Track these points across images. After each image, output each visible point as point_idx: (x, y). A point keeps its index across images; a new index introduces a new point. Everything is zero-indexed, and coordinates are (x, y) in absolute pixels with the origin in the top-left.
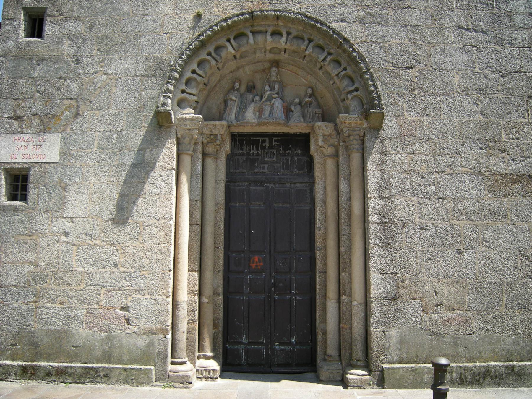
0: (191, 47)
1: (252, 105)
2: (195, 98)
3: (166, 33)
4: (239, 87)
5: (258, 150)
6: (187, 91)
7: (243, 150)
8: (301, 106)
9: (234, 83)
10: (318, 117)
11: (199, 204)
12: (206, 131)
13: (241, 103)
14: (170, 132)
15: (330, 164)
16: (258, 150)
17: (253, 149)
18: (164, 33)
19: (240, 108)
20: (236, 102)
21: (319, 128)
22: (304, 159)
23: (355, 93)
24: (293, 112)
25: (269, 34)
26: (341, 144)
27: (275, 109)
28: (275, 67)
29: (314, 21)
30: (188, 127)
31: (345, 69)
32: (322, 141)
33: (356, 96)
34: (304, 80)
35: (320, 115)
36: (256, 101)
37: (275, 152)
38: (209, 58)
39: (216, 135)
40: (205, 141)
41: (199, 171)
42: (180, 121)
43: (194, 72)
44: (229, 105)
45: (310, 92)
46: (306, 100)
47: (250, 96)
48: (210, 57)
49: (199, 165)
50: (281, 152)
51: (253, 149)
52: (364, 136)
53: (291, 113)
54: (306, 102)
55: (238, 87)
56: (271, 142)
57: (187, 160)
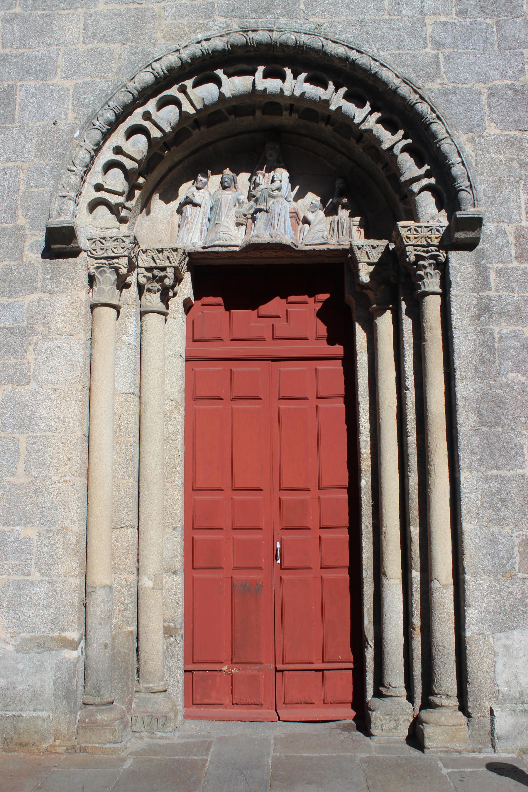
6: (105, 187)
39: (163, 269)
48: (148, 122)
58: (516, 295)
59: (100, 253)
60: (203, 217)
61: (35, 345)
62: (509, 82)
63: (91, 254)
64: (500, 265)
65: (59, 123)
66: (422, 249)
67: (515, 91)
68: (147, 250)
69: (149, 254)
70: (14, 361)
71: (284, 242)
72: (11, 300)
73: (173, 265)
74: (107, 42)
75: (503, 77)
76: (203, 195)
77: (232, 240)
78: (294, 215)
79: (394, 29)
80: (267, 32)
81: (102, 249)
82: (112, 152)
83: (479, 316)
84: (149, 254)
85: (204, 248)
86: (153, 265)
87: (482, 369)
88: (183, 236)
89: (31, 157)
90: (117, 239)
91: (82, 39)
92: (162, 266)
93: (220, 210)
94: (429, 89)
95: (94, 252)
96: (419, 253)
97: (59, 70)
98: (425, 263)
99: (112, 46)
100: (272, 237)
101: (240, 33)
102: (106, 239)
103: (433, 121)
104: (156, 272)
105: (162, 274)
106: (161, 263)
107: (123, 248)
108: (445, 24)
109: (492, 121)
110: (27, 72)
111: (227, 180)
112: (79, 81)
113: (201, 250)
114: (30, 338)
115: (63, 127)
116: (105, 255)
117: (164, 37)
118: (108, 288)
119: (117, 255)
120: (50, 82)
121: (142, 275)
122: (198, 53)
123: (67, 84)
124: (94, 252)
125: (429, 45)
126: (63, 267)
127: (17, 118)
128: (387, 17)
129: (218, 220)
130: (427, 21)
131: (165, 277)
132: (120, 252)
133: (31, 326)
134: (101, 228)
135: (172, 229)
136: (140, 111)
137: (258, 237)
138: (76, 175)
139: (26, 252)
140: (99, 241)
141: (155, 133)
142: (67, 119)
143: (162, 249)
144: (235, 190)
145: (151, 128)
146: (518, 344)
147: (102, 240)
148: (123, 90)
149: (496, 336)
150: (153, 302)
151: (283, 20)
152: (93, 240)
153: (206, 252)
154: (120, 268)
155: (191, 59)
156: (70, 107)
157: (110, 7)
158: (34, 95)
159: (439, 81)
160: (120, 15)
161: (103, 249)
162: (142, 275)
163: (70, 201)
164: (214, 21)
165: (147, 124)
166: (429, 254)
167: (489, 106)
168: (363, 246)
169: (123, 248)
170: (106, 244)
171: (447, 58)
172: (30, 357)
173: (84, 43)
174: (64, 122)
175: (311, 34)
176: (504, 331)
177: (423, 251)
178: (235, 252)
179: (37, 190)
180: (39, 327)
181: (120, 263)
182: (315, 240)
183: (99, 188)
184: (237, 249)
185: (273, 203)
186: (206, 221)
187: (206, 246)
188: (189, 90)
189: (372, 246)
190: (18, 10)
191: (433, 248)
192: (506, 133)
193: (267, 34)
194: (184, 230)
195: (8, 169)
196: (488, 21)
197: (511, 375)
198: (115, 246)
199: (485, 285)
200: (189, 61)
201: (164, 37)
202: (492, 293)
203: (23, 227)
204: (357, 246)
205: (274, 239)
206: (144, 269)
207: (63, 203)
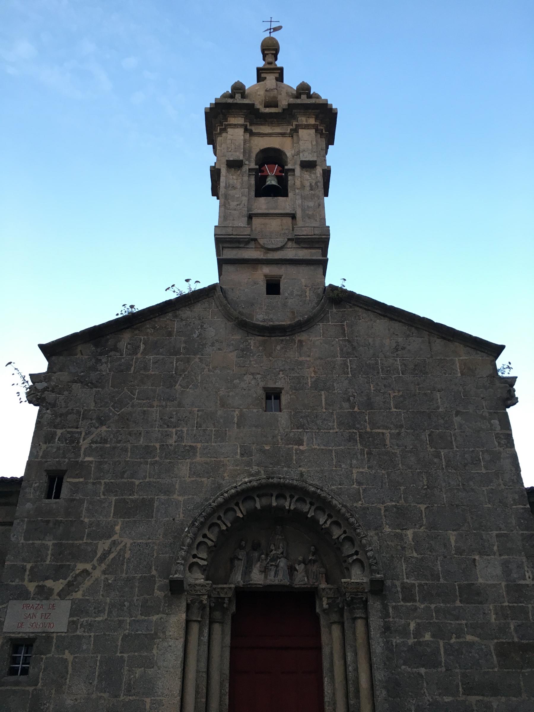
1: (258, 565)
2: (205, 563)
8: (306, 565)
10: (322, 577)
11: (205, 675)
12: (214, 595)
15: (336, 631)
19: (246, 568)
21: (324, 589)
23: (355, 557)
25: (274, 498)
26: (346, 608)
32: (327, 604)
33: (357, 559)
35: (324, 575)
36: (262, 560)
39: (224, 598)
40: (213, 605)
41: (205, 639)
46: (310, 558)
49: (206, 631)
52: (367, 601)
53: (296, 572)
57: (195, 628)
58: (403, 621)
59: (194, 592)
61: (158, 644)
62: (394, 503)
64: (394, 604)
65: (176, 519)
67: (398, 508)
70: (146, 654)
72: (146, 618)
74: (200, 477)
75: (392, 501)
79: (338, 475)
83: (385, 633)
87: (387, 663)
89: (161, 537)
91: (188, 475)
94: (356, 507)
97: (176, 491)
99: (203, 479)
108: (362, 473)
109: (387, 524)
110: (160, 491)
112: (186, 497)
114: (156, 640)
115: (177, 522)
117: (228, 476)
120: (171, 497)
123: (181, 498)
125: (355, 484)
127: (154, 515)
128: (335, 469)
130: (354, 471)
131: (224, 603)
132: (204, 591)
133: (156, 633)
136: (216, 515)
139: (156, 591)
141: (224, 528)
142: (179, 517)
146: (406, 649)
149: (394, 644)
151: (285, 469)
156: (181, 511)
157: (203, 459)
158: (163, 504)
159: (360, 502)
160: (206, 463)
164: (252, 468)
167: (385, 517)
171: (364, 490)
172: (155, 652)
174: (178, 519)
176: (398, 641)
177: (355, 595)
179: (163, 555)
180: (161, 635)
186: (245, 568)
188: (240, 505)
190: (157, 459)
192: (394, 531)
195: (149, 543)
196: (383, 472)
197: (403, 667)
199: (387, 615)
201: (228, 476)
202: (391, 619)
203: (155, 576)
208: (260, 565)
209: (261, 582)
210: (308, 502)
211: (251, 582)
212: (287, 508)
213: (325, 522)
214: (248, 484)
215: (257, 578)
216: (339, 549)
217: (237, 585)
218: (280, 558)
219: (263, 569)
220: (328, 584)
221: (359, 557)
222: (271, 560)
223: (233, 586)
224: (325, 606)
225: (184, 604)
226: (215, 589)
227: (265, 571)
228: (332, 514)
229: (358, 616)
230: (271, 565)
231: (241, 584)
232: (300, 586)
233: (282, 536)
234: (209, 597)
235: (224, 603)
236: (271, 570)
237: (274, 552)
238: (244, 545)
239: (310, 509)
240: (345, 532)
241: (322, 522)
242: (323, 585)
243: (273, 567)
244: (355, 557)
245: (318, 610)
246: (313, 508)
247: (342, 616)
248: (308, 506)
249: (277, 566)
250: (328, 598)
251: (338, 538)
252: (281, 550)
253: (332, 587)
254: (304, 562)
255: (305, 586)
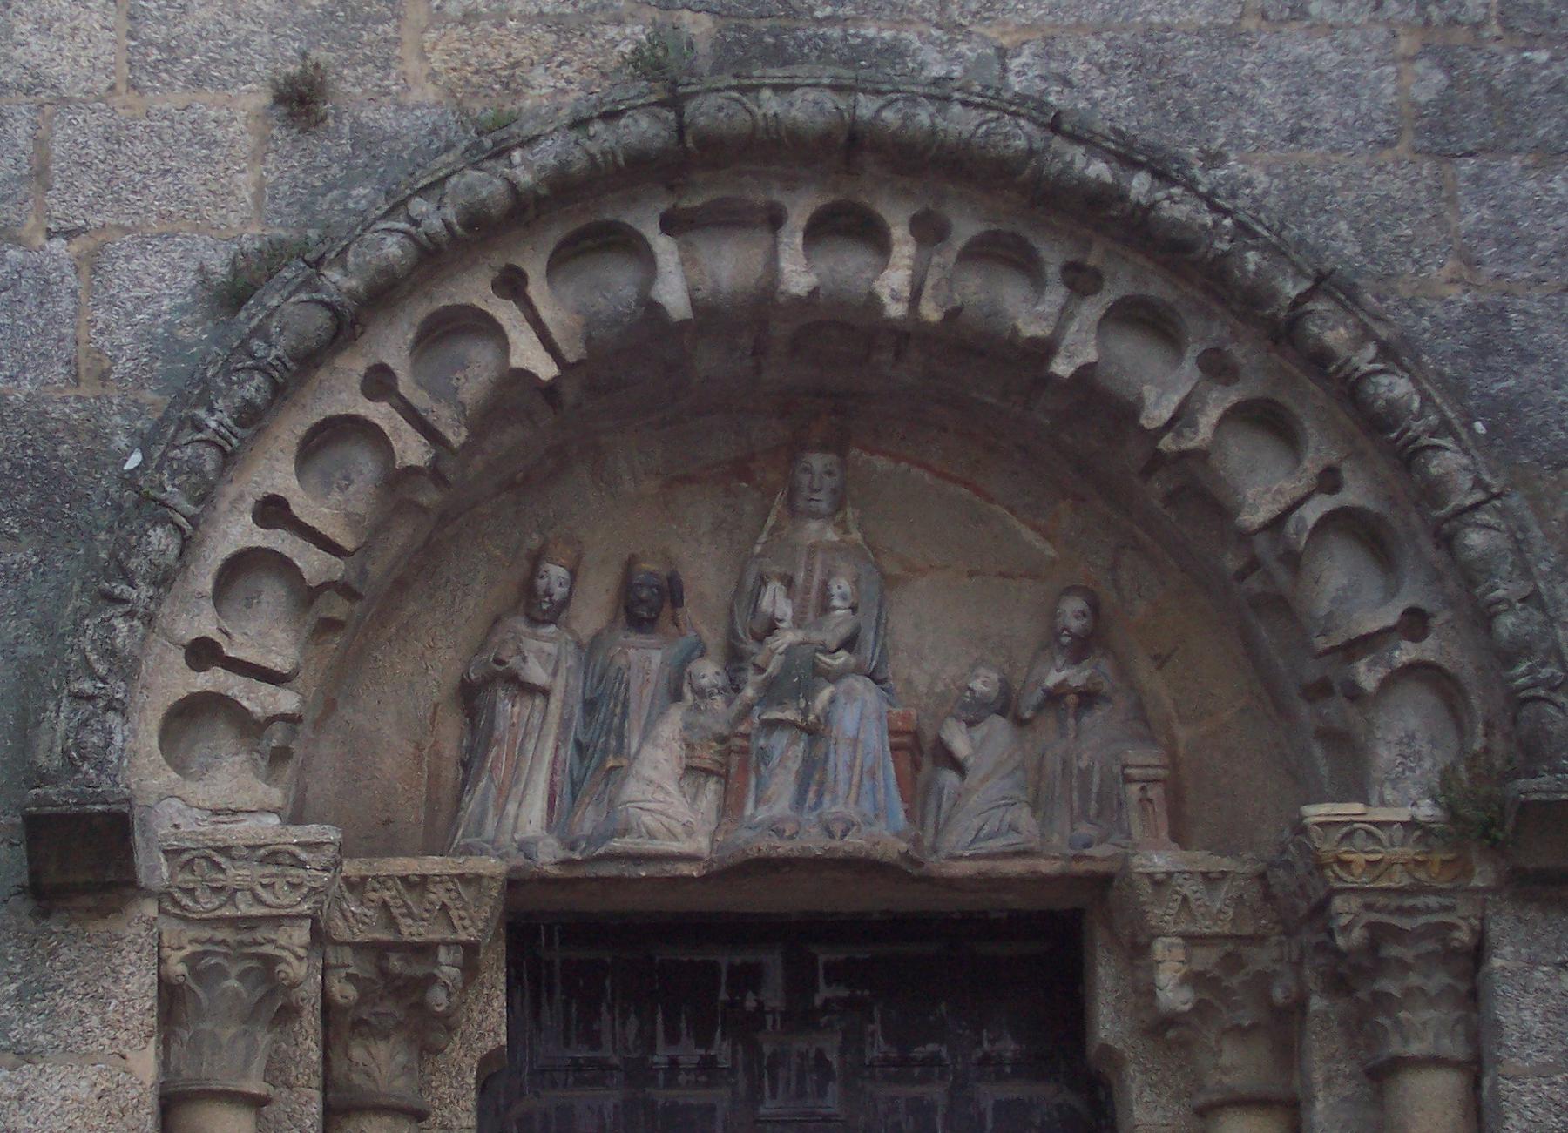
0: (257, 345)
1: (671, 726)
3: (69, 234)
4: (570, 593)
5: (705, 1040)
7: (594, 1041)
8: (1020, 722)
9: (537, 559)
10: (1145, 801)
12: (356, 922)
13: (590, 706)
14: (113, 943)
16: (705, 1040)
17: (673, 1037)
18: (50, 235)
19: (579, 745)
20: (555, 704)
21: (1160, 883)
22: (1047, 1096)
24: (958, 766)
25: (792, 240)
26: (1317, 1003)
27: (840, 757)
28: (824, 447)
29: (1109, 156)
30: (245, 908)
31: (1329, 480)
33: (1414, 670)
34: (1028, 535)
35: (1155, 792)
36: (700, 693)
37: (833, 1057)
38: (379, 413)
40: (344, 992)
42: (189, 865)
43: (273, 511)
44: (501, 724)
45: (1075, 624)
46: (1053, 679)
47: (646, 658)
50: (878, 1048)
51: (673, 1037)
52: (1478, 953)
53: (949, 778)
54: (1054, 697)
55: (559, 592)
56: (800, 981)
59: (207, 903)
60: (557, 739)
63: (176, 903)
66: (1394, 902)
68: (364, 879)
69: (373, 895)
71: (877, 853)
73: (463, 936)
76: (549, 647)
77: (673, 836)
78: (906, 739)
80: (828, 93)
81: (217, 890)
82: (249, 518)
84: (373, 895)
85: (567, 863)
86: (385, 936)
88: (484, 813)
90: (274, 853)
92: (417, 939)
93: (624, 715)
95: (186, 901)
96: (1385, 918)
98: (1406, 953)
100: (831, 835)
101: (735, 95)
102: (234, 853)
103: (1436, 441)
104: (395, 963)
105: (419, 970)
106: (414, 930)
107: (294, 886)
111: (644, 594)
113: (555, 871)
116: (227, 912)
118: (232, 1031)
119: (274, 912)
121: (343, 973)
122: (579, 161)
124: (186, 901)
126: (66, 954)
129: (620, 750)
131: (432, 979)
132: (285, 899)
134: (216, 812)
135: (434, 778)
136: (354, 365)
137: (779, 833)
138: (131, 615)
140: (208, 858)
141: (412, 450)
143: (424, 877)
144: (673, 630)
145: (395, 429)
147: (219, 859)
148: (303, 296)
150: (376, 1074)
152: (186, 856)
153: (578, 880)
154: (280, 960)
155: (551, 186)
161: (223, 888)
162: (343, 973)
163: (110, 715)
165: (379, 413)
166: (1422, 920)
168: (1169, 874)
169: (293, 886)
170: (232, 872)
173: (134, 87)
175: (989, 107)
177: (1401, 911)
178: (690, 879)
181: (282, 942)
182: (990, 837)
183: (203, 653)
184: (693, 871)
185: (832, 700)
186: (569, 750)
187: (577, 856)
188: (537, 289)
189: (1205, 875)
191: (1433, 901)
193: (830, 101)
194: (487, 789)
198: (265, 881)
200: (543, 191)
204: (1150, 875)
205: (836, 843)
206: (348, 951)
207: (84, 724)
208: (688, 727)
209: (700, 844)
210: (1053, 257)
211: (618, 844)
212: (896, 310)
213: (1182, 417)
214: (597, 127)
215: (667, 812)
216: (1280, 606)
217: (520, 860)
218: (834, 677)
219: (708, 756)
220: (1184, 847)
221: (1426, 650)
222: (772, 691)
223: (490, 865)
224: (1173, 995)
225: (139, 984)
226: (356, 886)
227: (726, 766)
228: (1238, 352)
229: (1415, 1049)
230: (772, 726)
231: (549, 855)
232: (984, 865)
233: (843, 526)
234: (320, 937)
235: (432, 979)
236: (764, 755)
237: (787, 637)
238: (559, 592)
239: (1065, 315)
240: (1329, 480)
241: (1158, 411)
242: (1160, 861)
243: (780, 740)
244: (1405, 653)
245: (1109, 1024)
246: (1091, 310)
247: (1288, 1052)
248: (1055, 296)
249: (814, 732)
250: (1192, 940)
251: (1277, 523)
252: (840, 621)
253: (1226, 864)
254: (1005, 704)
255: (1016, 867)
